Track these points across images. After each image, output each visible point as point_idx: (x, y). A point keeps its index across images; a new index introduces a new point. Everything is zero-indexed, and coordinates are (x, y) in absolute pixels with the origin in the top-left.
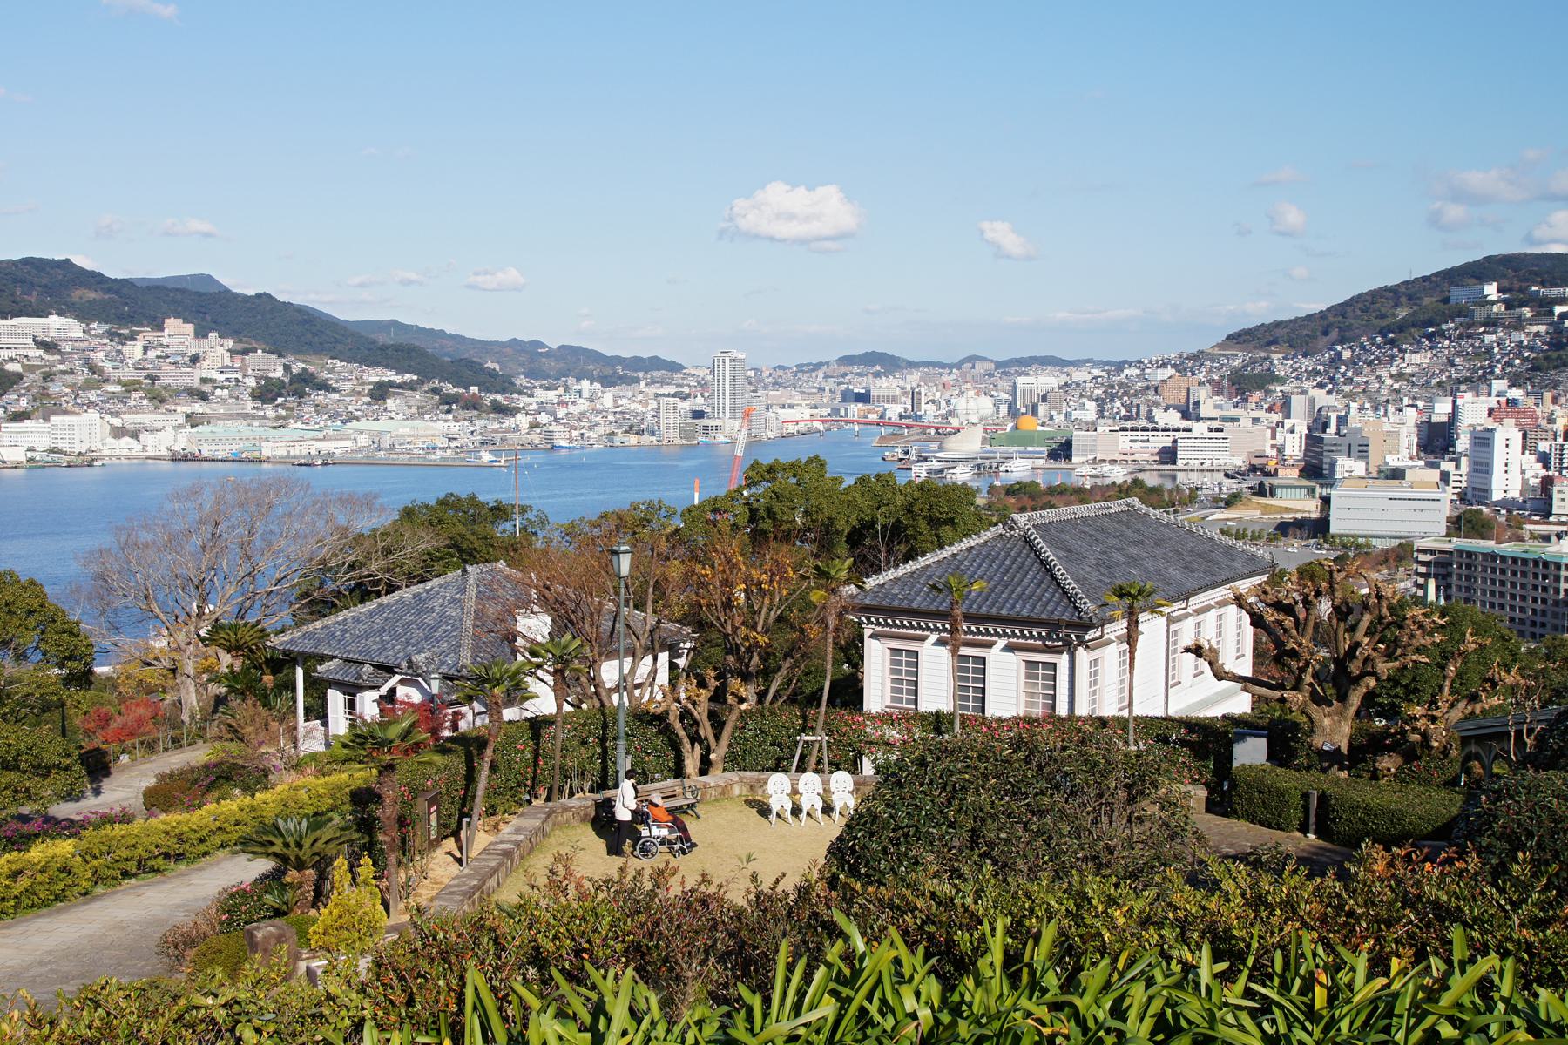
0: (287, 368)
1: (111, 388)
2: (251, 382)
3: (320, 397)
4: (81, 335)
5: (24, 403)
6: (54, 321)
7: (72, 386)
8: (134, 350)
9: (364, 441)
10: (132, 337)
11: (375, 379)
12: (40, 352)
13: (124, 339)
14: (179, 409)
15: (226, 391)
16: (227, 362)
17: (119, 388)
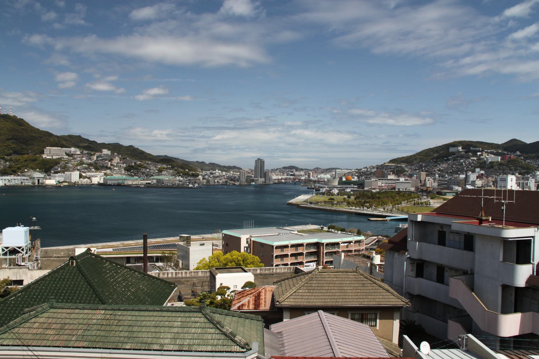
0: (135, 163)
1: (84, 166)
2: (125, 165)
3: (143, 170)
4: (79, 153)
5: (59, 169)
6: (73, 149)
7: (73, 165)
8: (95, 158)
9: (155, 181)
10: (94, 155)
11: (159, 167)
12: (67, 157)
13: (91, 155)
14: (103, 172)
15: (117, 168)
16: (119, 161)
17: (86, 166)
